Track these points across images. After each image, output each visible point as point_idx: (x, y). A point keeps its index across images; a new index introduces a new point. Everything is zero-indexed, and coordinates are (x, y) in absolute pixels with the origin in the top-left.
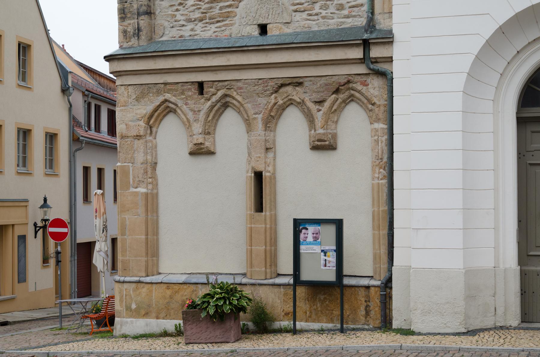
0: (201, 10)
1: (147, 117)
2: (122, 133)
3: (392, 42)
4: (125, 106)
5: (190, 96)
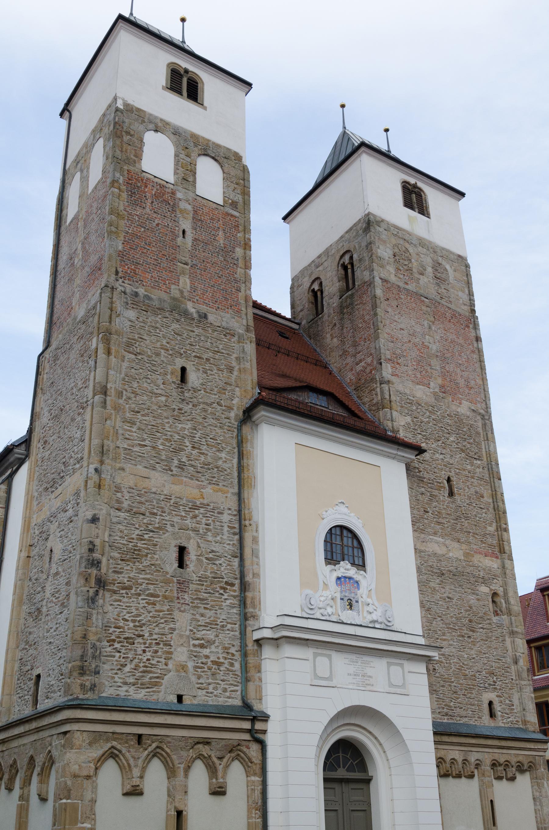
0: (135, 677)
1: (97, 760)
2: (75, 773)
3: (267, 721)
4: (79, 749)
5: (132, 745)
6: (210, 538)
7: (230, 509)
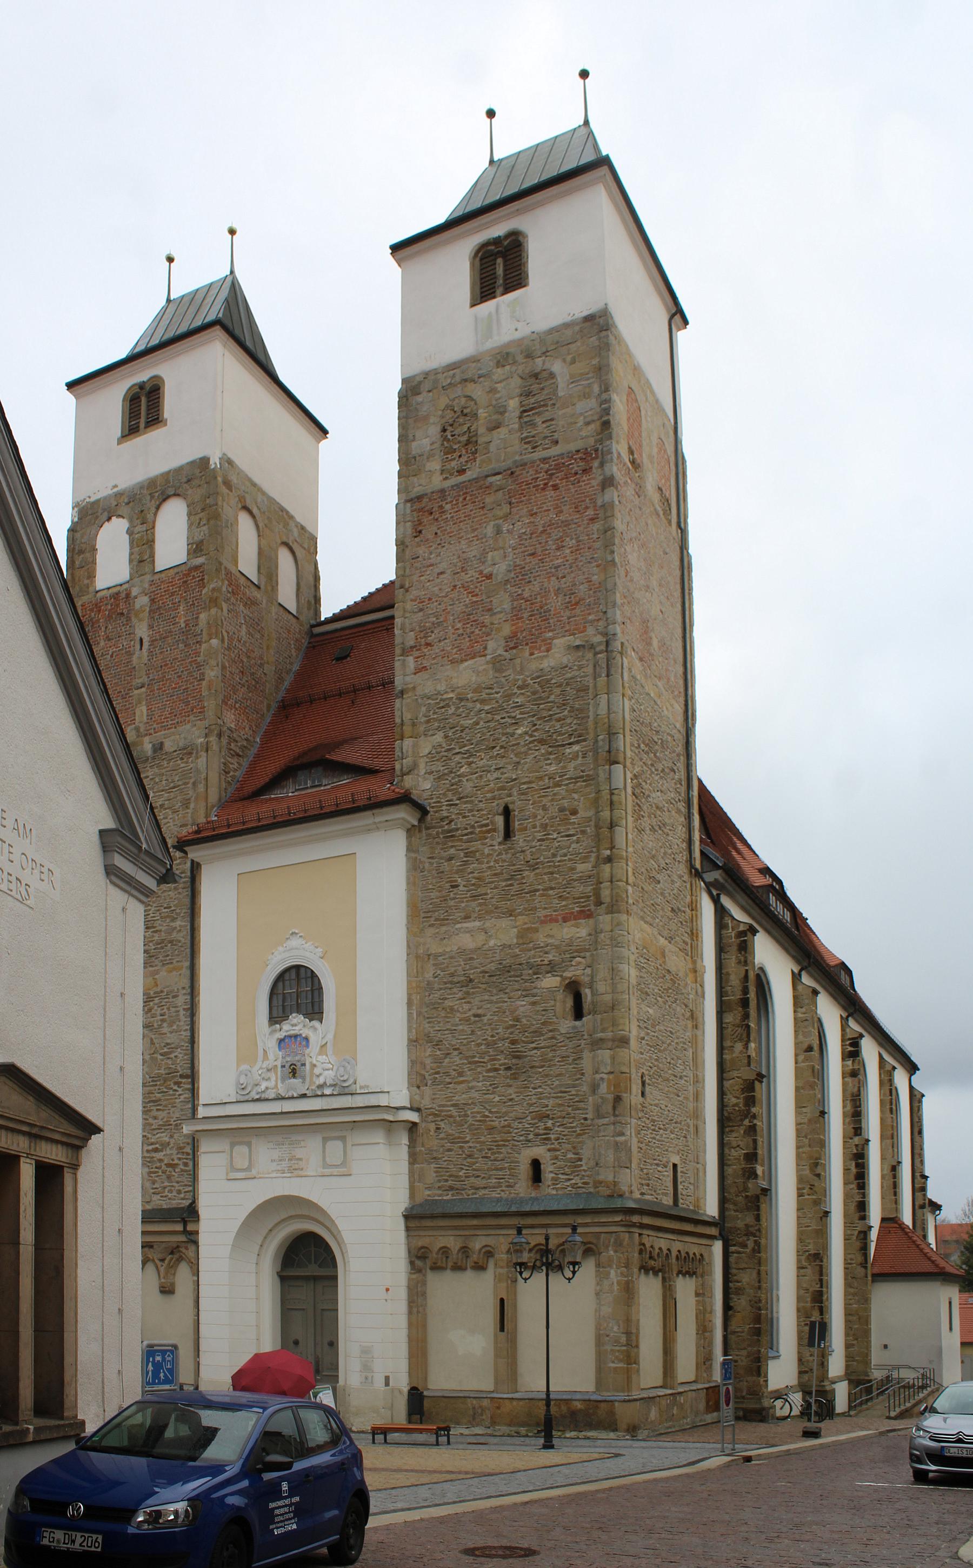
7: (184, 988)
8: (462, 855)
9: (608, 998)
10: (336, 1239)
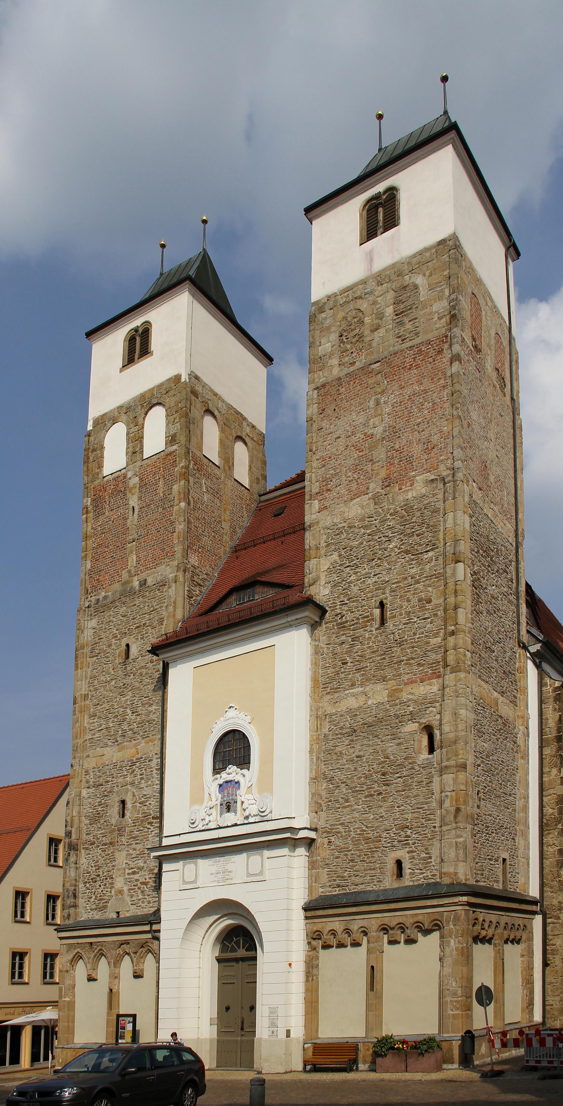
6: (142, 786)
7: (156, 754)
8: (350, 640)
9: (452, 735)
10: (256, 929)
